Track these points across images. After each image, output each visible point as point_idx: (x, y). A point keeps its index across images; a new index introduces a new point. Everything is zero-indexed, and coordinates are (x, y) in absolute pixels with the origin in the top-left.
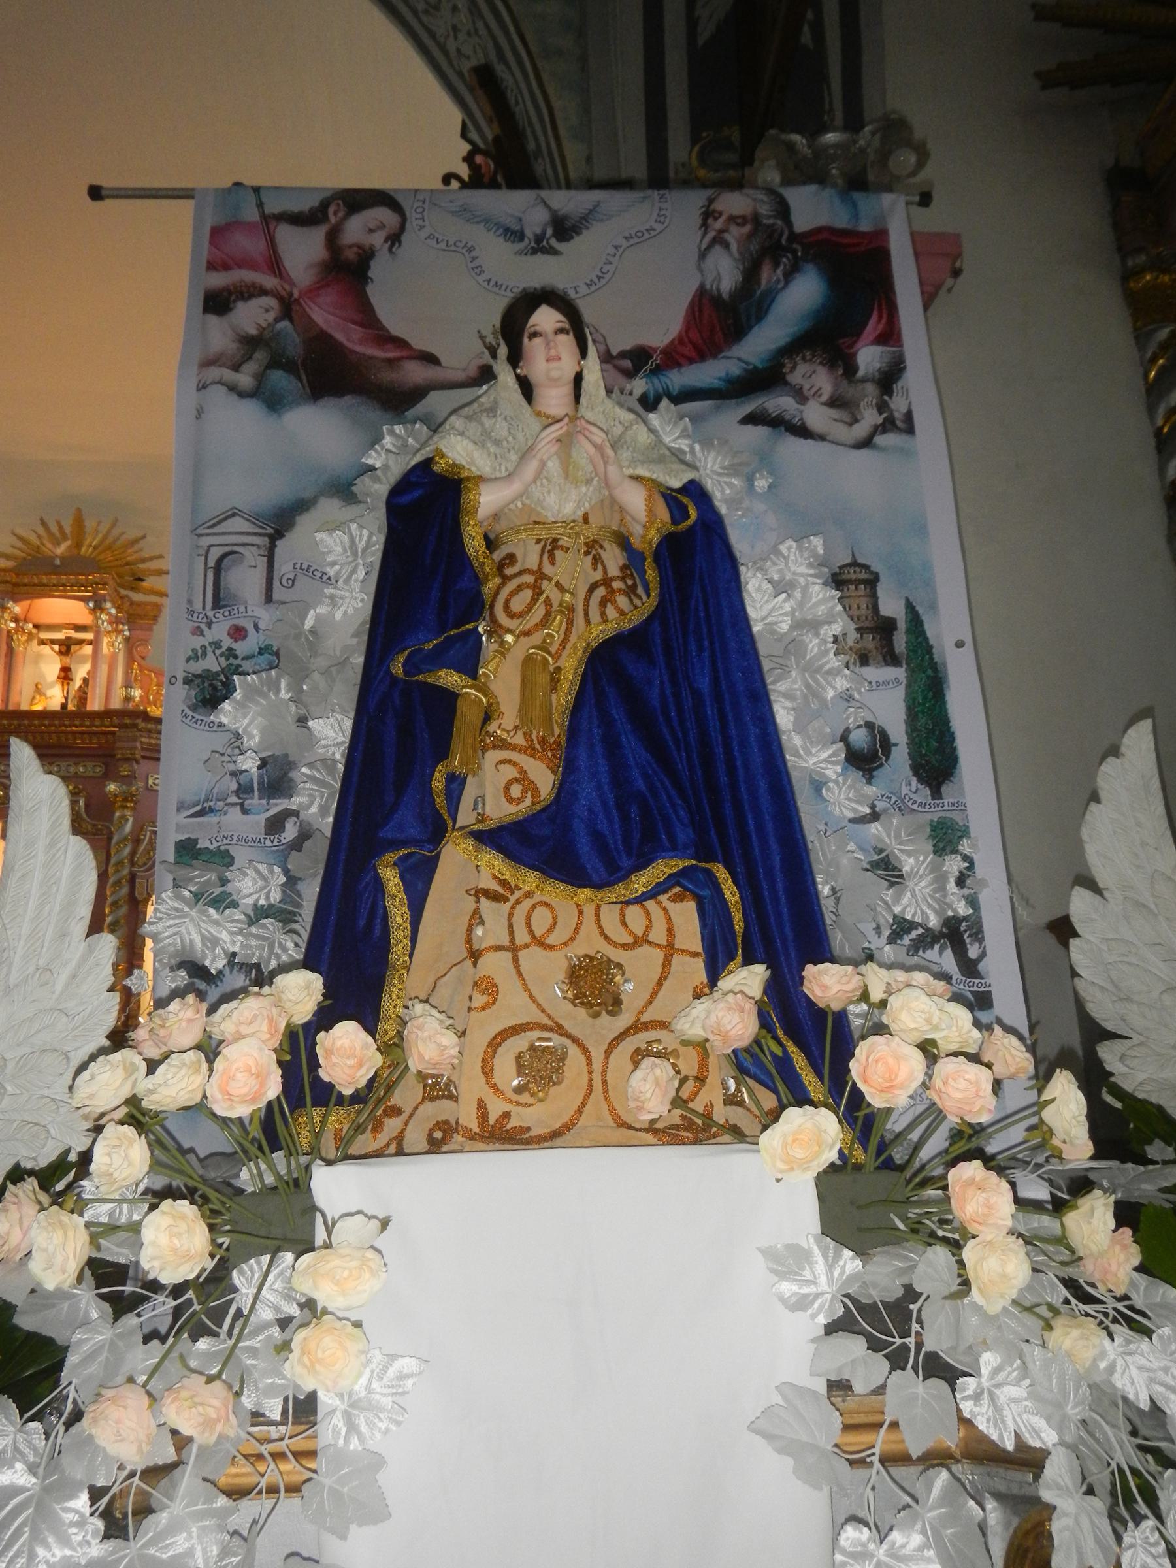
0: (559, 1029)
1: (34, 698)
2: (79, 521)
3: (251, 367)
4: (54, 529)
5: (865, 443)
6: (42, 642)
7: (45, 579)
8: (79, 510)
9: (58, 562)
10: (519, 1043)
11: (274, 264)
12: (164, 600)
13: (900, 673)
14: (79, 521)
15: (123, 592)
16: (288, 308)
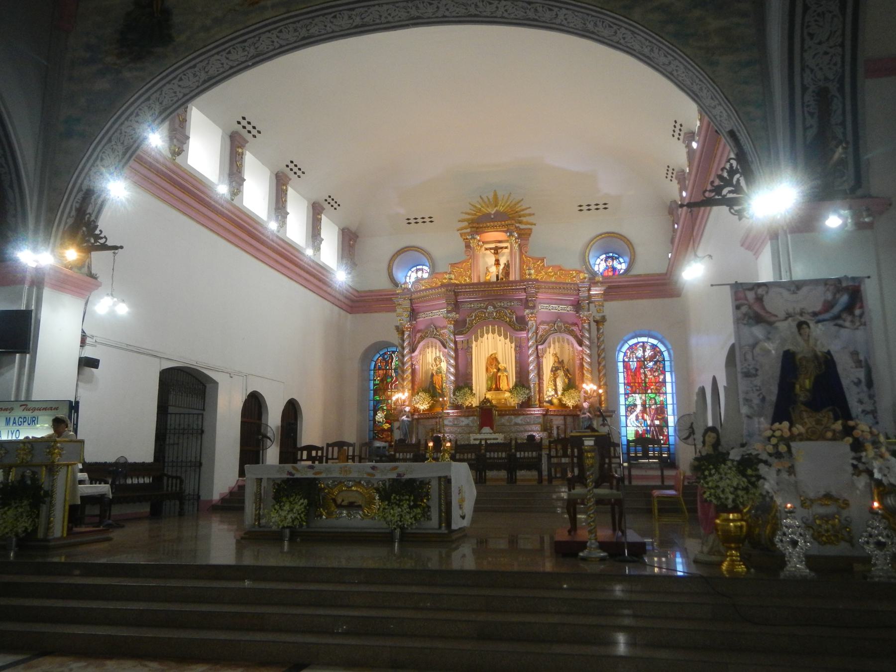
0: (814, 427)
1: (486, 273)
2: (495, 195)
3: (746, 319)
4: (486, 199)
5: (857, 329)
6: (486, 249)
7: (488, 224)
8: (495, 191)
9: (492, 217)
10: (810, 430)
11: (746, 299)
12: (533, 227)
13: (863, 369)
14: (495, 195)
15: (517, 225)
16: (750, 307)
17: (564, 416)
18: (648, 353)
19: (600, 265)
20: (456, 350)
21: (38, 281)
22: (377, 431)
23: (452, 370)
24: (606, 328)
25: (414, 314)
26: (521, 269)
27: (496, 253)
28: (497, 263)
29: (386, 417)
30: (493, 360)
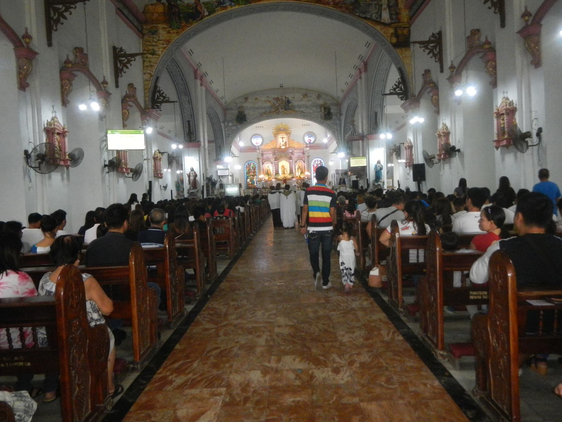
2: (282, 122)
14: (282, 122)
17: (301, 180)
18: (319, 162)
19: (307, 139)
20: (275, 165)
21: (227, 164)
22: (247, 184)
23: (274, 170)
24: (310, 158)
25: (262, 155)
26: (289, 143)
27: (283, 139)
28: (283, 141)
29: (250, 180)
30: (283, 167)
